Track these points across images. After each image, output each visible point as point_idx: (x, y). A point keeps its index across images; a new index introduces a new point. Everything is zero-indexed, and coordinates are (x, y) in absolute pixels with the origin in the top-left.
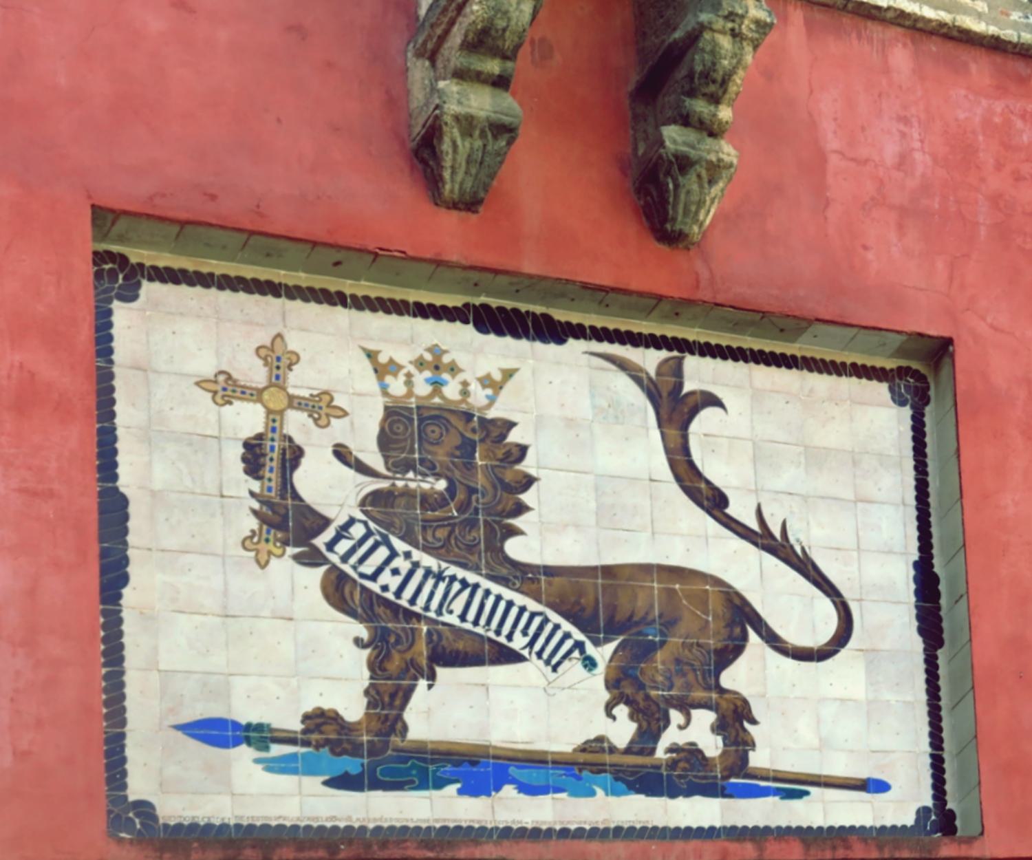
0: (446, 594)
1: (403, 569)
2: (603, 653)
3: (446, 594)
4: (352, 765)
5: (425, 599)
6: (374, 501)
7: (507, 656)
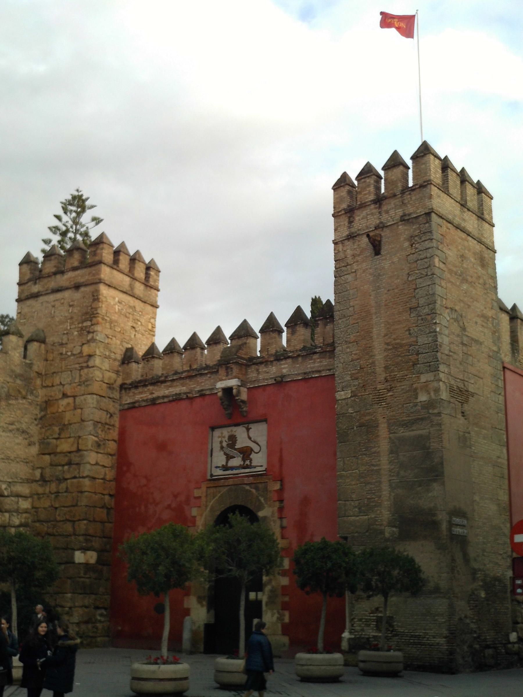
2: (241, 456)
6: (228, 445)
7: (235, 457)
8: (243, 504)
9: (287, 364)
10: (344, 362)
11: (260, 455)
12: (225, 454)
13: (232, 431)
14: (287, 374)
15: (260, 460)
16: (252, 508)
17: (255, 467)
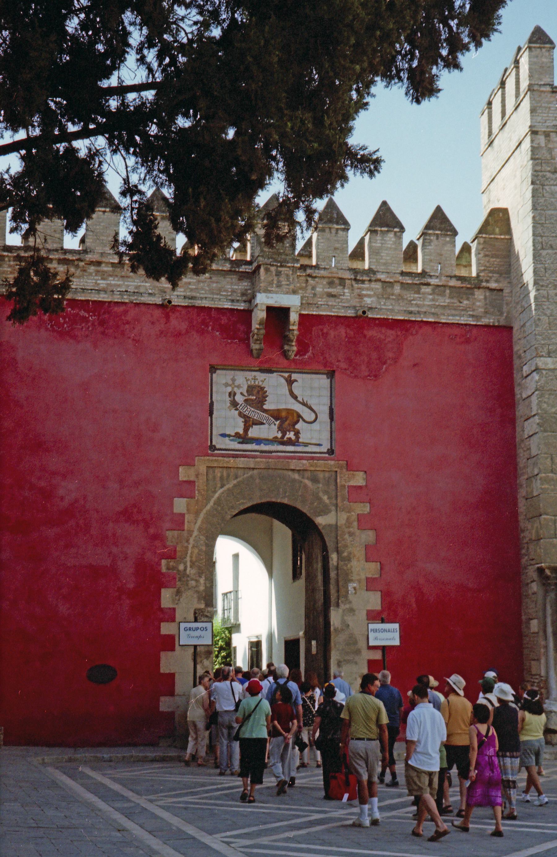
0: (255, 414)
1: (250, 411)
3: (255, 414)
4: (241, 440)
5: (252, 415)
6: (246, 401)
7: (262, 424)
8: (286, 501)
9: (372, 289)
10: (551, 315)
11: (316, 426)
12: (240, 414)
13: (255, 379)
14: (374, 306)
15: (315, 434)
16: (305, 510)
17: (306, 445)
